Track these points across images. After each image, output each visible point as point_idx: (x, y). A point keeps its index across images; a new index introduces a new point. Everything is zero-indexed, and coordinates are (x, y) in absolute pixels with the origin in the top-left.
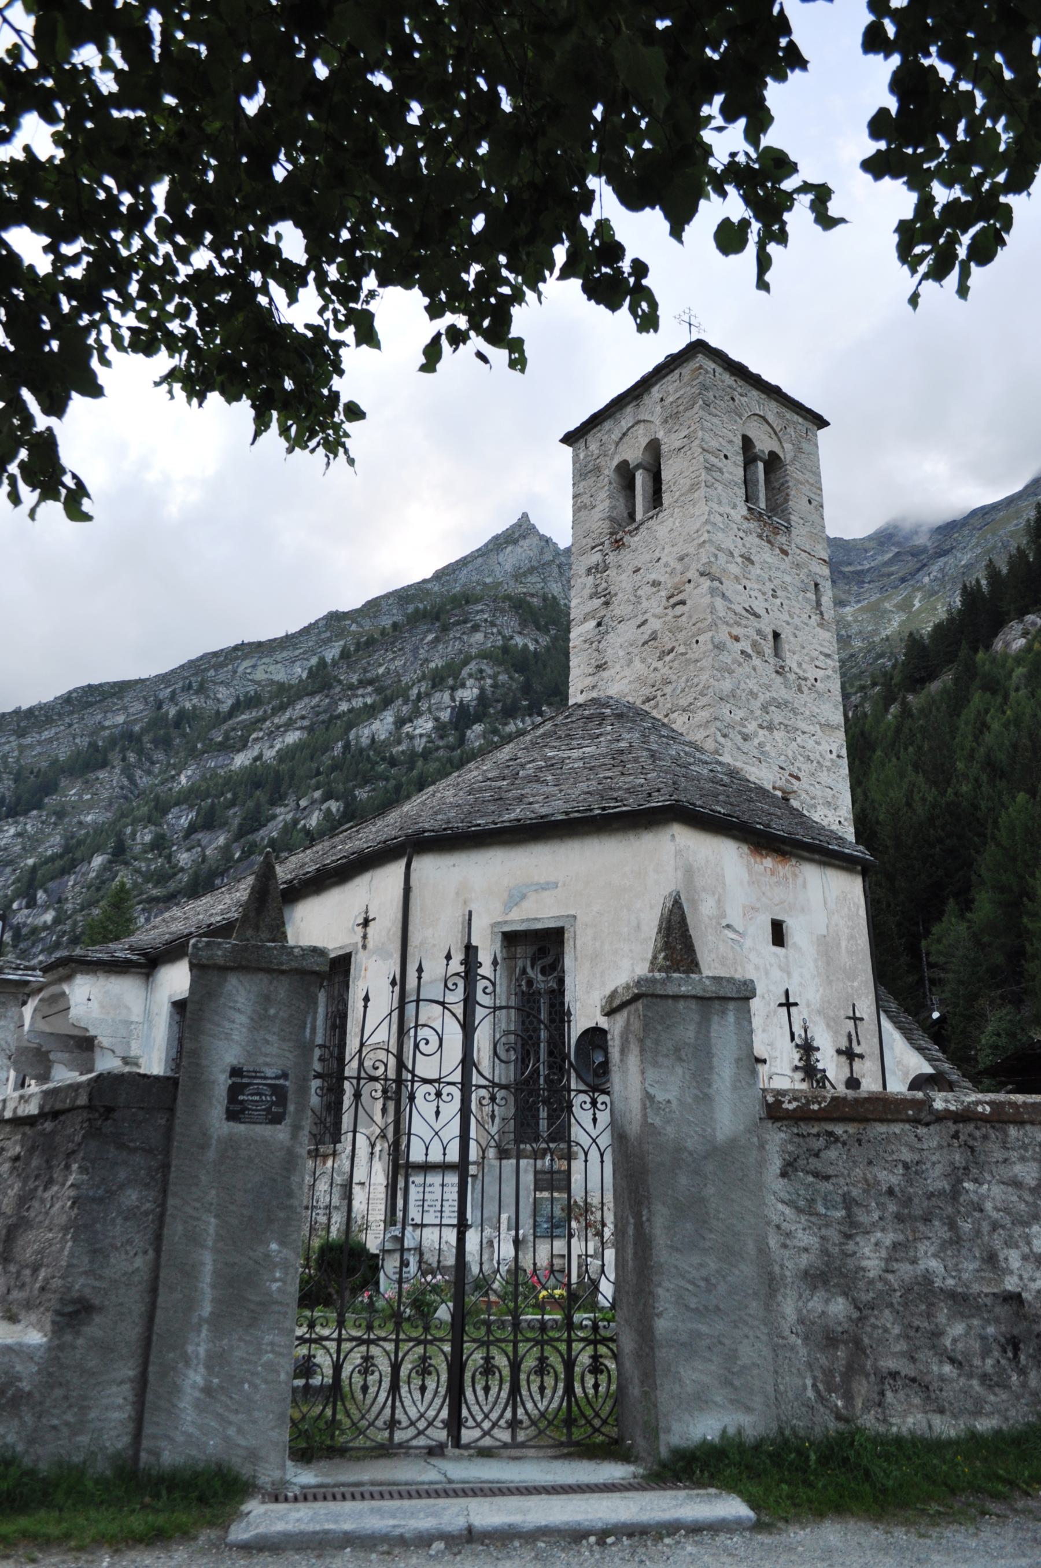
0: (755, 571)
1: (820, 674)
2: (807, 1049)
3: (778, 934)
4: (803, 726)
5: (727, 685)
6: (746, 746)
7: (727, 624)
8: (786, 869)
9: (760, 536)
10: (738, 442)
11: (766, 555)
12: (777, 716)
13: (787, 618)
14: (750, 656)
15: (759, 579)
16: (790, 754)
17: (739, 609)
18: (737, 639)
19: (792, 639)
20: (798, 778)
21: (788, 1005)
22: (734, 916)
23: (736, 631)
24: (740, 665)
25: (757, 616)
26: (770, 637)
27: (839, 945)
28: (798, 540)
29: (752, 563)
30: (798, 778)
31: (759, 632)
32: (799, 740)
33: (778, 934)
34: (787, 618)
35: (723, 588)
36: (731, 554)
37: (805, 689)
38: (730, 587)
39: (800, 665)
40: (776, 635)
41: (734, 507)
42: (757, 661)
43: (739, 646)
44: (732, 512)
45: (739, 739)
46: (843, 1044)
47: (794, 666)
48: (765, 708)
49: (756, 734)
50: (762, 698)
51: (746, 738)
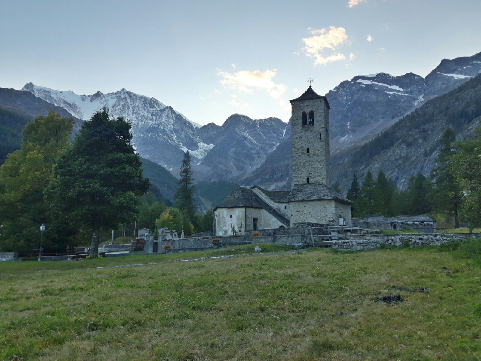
0: (303, 139)
1: (319, 151)
2: (234, 228)
3: (231, 217)
4: (313, 163)
5: (295, 163)
6: (298, 172)
7: (295, 152)
8: (233, 210)
9: (305, 131)
10: (301, 114)
11: (307, 134)
12: (306, 164)
13: (311, 144)
14: (301, 155)
15: (304, 140)
16: (309, 169)
17: (298, 148)
18: (298, 153)
19: (312, 148)
20: (311, 174)
21: (231, 224)
22: (225, 216)
23: (298, 152)
24: (298, 158)
25: (303, 147)
26: (306, 150)
27: (240, 216)
28: (316, 127)
29: (302, 137)
30: (311, 174)
31: (303, 150)
32: (312, 166)
33: (231, 217)
34: (311, 144)
35: (295, 146)
36: (297, 138)
37: (315, 156)
38: (296, 145)
39: (314, 152)
40: (308, 150)
41: (298, 129)
42: (302, 156)
43: (298, 154)
44: (298, 130)
45: (297, 171)
46: (239, 227)
47: (312, 153)
48: (304, 164)
49: (301, 169)
50: (303, 162)
51: (298, 170)
